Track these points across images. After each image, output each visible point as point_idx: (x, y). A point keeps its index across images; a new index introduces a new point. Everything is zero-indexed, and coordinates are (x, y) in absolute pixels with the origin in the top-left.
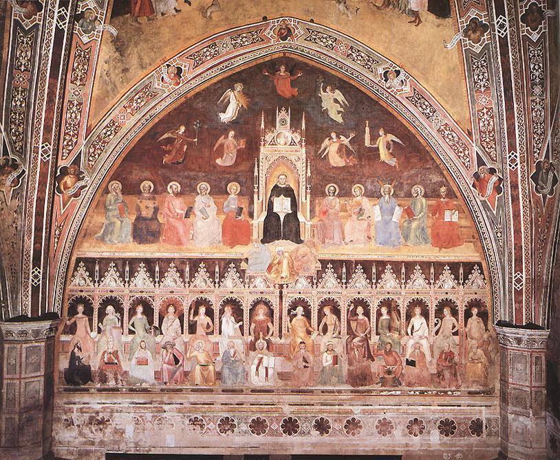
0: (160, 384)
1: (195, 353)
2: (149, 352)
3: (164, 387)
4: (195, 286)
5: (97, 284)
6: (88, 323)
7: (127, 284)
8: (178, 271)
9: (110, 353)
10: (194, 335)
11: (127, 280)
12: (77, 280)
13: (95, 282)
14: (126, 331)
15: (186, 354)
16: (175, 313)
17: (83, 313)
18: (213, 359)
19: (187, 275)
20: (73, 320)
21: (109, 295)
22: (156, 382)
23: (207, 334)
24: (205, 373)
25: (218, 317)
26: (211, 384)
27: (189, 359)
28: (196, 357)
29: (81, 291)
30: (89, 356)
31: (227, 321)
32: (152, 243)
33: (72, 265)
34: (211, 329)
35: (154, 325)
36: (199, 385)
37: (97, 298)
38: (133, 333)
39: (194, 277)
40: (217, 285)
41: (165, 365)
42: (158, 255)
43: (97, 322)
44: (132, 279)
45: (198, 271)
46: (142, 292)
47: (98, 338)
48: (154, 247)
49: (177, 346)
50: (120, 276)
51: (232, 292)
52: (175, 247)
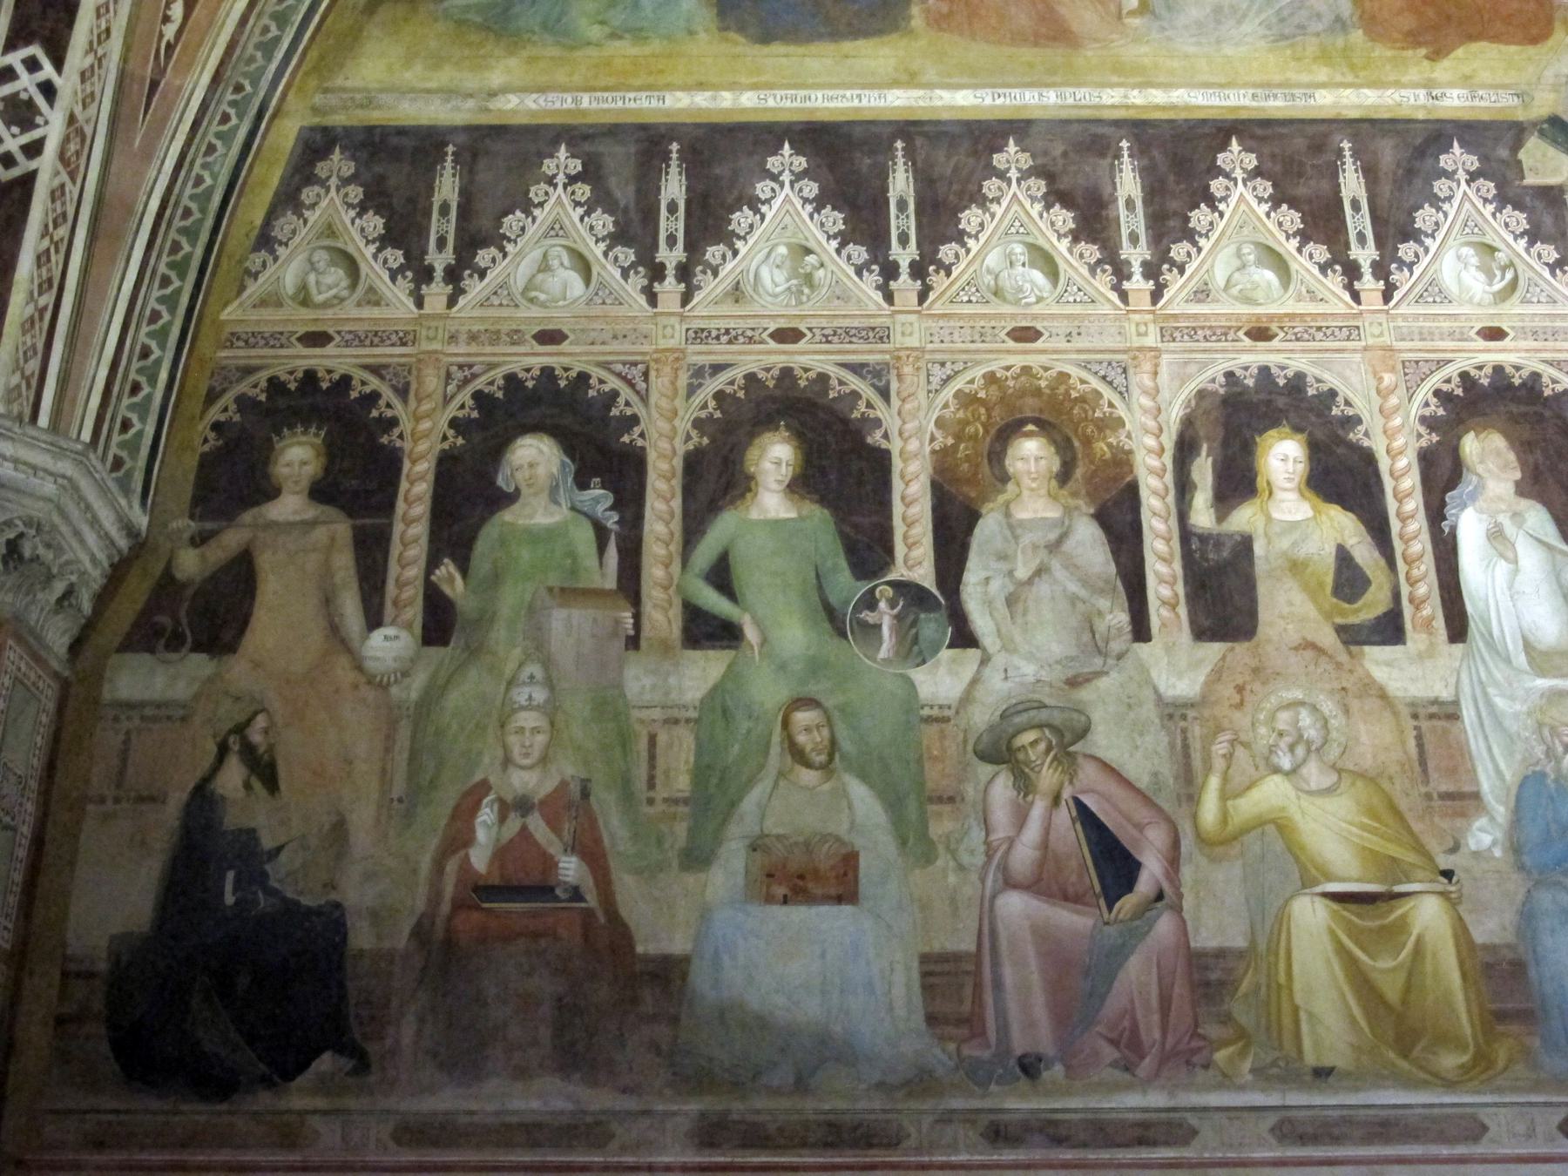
0: (977, 1075)
1: (1272, 793)
2: (858, 791)
3: (1018, 1103)
4: (1202, 293)
5: (437, 292)
6: (344, 563)
7: (670, 287)
8: (1057, 196)
9: (523, 805)
10: (1241, 648)
11: (670, 257)
12: (288, 271)
13: (425, 275)
14: (663, 618)
15: (1192, 798)
16: (1064, 476)
17: (321, 492)
18: (1434, 846)
19: (1131, 221)
20: (232, 540)
21: (529, 360)
22: (939, 1056)
23: (1352, 636)
24: (1385, 967)
25: (1415, 504)
26: (1450, 1061)
27: (1218, 844)
28: (1279, 825)
29: (317, 339)
30: (339, 831)
31: (1496, 535)
32: (856, 33)
33: (269, 176)
34: (1373, 605)
35: (899, 572)
36: (1356, 1078)
37: (432, 382)
38: (723, 634)
39: (1190, 235)
40: (1369, 284)
41: (1014, 904)
42: (897, 101)
43: (418, 551)
44: (713, 253)
45: (1211, 201)
46: (787, 335)
47: (418, 681)
48: (877, 54)
49: (1105, 741)
50: (619, 237)
51: (1494, 334)
52: (1027, 54)
